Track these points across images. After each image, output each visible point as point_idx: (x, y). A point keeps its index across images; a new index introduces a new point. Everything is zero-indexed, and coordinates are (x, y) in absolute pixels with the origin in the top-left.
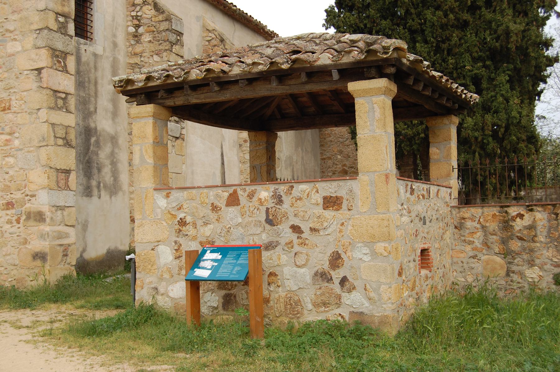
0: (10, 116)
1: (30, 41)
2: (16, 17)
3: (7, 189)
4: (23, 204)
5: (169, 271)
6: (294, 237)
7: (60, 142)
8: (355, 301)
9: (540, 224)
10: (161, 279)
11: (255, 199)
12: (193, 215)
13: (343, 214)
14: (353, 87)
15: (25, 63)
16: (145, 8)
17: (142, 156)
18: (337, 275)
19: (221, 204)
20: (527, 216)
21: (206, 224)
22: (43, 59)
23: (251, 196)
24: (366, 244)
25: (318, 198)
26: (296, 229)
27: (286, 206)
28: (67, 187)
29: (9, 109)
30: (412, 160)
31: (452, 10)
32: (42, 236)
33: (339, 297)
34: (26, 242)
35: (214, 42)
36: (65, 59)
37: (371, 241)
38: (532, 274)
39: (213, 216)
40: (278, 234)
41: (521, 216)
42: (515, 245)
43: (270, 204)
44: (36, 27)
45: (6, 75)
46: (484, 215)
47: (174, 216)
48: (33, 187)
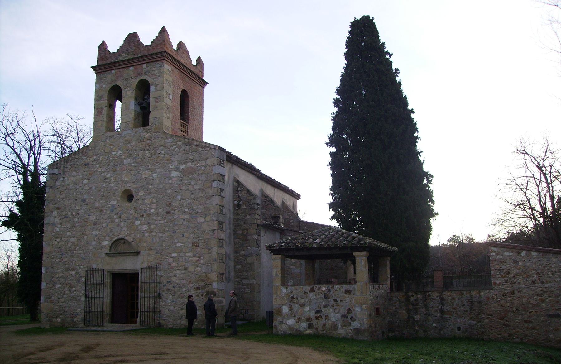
0: (199, 249)
5: (287, 315)
6: (334, 303)
7: (221, 261)
8: (355, 324)
16: (243, 193)
17: (276, 274)
19: (308, 291)
20: (415, 296)
21: (302, 298)
22: (215, 226)
23: (319, 289)
25: (343, 290)
26: (335, 301)
27: (331, 293)
28: (222, 281)
29: (198, 246)
30: (374, 278)
33: (350, 323)
35: (268, 202)
36: (222, 224)
37: (361, 304)
39: (305, 295)
41: (413, 296)
42: (411, 307)
43: (326, 292)
46: (399, 296)
47: (290, 296)
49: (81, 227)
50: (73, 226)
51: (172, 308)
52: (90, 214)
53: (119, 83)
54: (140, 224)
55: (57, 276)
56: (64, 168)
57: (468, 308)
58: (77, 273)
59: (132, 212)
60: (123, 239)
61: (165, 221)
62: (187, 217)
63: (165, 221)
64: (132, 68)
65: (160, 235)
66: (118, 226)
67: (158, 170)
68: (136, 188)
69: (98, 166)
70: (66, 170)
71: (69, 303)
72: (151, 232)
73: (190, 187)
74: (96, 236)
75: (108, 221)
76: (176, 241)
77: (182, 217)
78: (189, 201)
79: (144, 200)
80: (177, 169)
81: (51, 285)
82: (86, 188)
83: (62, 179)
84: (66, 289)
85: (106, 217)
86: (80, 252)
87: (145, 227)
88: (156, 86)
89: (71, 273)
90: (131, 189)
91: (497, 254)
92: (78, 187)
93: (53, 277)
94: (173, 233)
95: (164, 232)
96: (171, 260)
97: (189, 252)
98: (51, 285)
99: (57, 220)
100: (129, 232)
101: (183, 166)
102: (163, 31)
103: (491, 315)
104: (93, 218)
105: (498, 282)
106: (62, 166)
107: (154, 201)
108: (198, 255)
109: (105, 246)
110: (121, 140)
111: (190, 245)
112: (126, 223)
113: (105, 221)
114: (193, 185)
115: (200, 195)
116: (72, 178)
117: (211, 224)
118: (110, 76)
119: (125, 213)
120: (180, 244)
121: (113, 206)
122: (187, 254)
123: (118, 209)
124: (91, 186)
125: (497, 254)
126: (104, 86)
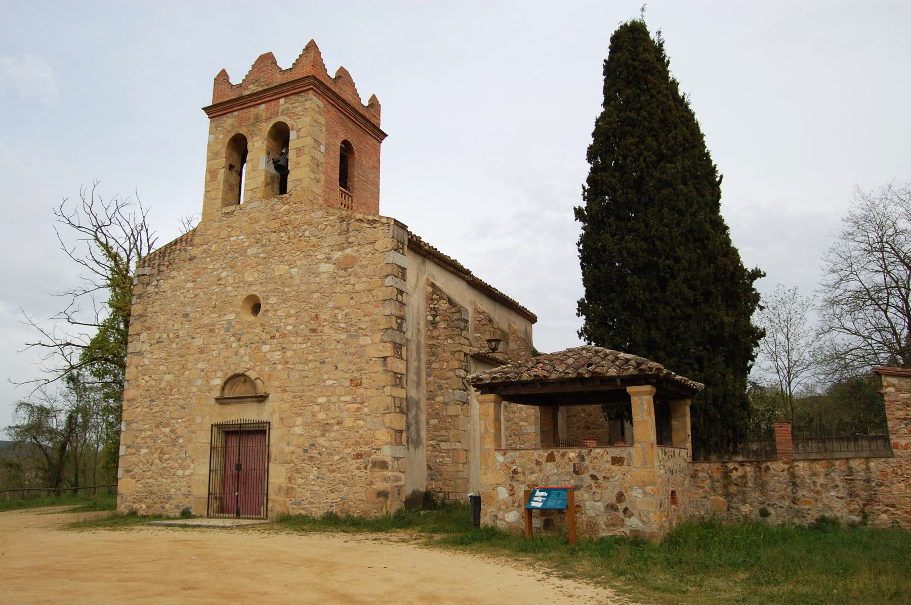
0: (361, 390)
1: (378, 337)
2: (367, 319)
3: (357, 443)
4: (370, 455)
5: (506, 504)
6: (592, 482)
7: (398, 410)
8: (633, 522)
9: (749, 475)
10: (499, 509)
11: (566, 458)
12: (522, 467)
13: (625, 468)
14: (629, 389)
15: (374, 352)
16: (441, 302)
18: (621, 507)
19: (543, 460)
20: (740, 469)
21: (532, 473)
22: (388, 350)
23: (563, 455)
24: (640, 487)
26: (594, 477)
27: (587, 462)
28: (401, 444)
31: (679, 306)
32: (385, 479)
33: (623, 520)
34: (372, 483)
35: (485, 322)
36: (401, 349)
37: (642, 486)
38: (745, 509)
39: (537, 468)
40: (582, 480)
41: (736, 469)
42: (733, 489)
44: (382, 327)
45: (358, 360)
46: (710, 469)
47: (509, 468)
48: (378, 443)
49: (182, 357)
50: (170, 355)
51: (318, 488)
52: (195, 335)
53: (243, 131)
54: (269, 351)
55: (143, 435)
56: (159, 265)
57: (843, 493)
58: (172, 431)
59: (257, 331)
60: (243, 375)
61: (309, 344)
62: (343, 336)
63: (309, 344)
64: (263, 106)
65: (300, 367)
66: (236, 354)
67: (298, 263)
68: (265, 292)
69: (208, 259)
70: (163, 268)
71: (160, 479)
72: (286, 363)
73: (348, 287)
74: (202, 370)
75: (222, 346)
76: (325, 377)
77: (337, 337)
78: (347, 311)
79: (276, 311)
80: (328, 259)
81: (133, 450)
82: (190, 295)
83: (155, 283)
84: (156, 456)
85: (219, 339)
86: (177, 396)
87: (277, 355)
88: (298, 131)
89: (163, 430)
90: (257, 294)
91: (899, 390)
92: (178, 293)
93: (136, 437)
94: (321, 363)
95: (307, 361)
96: (317, 408)
97: (346, 395)
98: (133, 450)
99: (146, 347)
100: (252, 364)
101: (337, 255)
102: (312, 47)
103: (893, 506)
104: (199, 342)
105: (903, 442)
106: (157, 262)
107: (293, 312)
108: (359, 400)
109: (215, 386)
110: (245, 219)
111: (348, 383)
112: (248, 350)
113: (216, 347)
114: (354, 285)
115: (365, 300)
116: (170, 281)
117: (380, 348)
118: (230, 122)
119: (248, 333)
120: (332, 382)
121: (229, 322)
122: (342, 399)
123: (238, 327)
124: (197, 291)
125: (899, 390)
126: (221, 136)
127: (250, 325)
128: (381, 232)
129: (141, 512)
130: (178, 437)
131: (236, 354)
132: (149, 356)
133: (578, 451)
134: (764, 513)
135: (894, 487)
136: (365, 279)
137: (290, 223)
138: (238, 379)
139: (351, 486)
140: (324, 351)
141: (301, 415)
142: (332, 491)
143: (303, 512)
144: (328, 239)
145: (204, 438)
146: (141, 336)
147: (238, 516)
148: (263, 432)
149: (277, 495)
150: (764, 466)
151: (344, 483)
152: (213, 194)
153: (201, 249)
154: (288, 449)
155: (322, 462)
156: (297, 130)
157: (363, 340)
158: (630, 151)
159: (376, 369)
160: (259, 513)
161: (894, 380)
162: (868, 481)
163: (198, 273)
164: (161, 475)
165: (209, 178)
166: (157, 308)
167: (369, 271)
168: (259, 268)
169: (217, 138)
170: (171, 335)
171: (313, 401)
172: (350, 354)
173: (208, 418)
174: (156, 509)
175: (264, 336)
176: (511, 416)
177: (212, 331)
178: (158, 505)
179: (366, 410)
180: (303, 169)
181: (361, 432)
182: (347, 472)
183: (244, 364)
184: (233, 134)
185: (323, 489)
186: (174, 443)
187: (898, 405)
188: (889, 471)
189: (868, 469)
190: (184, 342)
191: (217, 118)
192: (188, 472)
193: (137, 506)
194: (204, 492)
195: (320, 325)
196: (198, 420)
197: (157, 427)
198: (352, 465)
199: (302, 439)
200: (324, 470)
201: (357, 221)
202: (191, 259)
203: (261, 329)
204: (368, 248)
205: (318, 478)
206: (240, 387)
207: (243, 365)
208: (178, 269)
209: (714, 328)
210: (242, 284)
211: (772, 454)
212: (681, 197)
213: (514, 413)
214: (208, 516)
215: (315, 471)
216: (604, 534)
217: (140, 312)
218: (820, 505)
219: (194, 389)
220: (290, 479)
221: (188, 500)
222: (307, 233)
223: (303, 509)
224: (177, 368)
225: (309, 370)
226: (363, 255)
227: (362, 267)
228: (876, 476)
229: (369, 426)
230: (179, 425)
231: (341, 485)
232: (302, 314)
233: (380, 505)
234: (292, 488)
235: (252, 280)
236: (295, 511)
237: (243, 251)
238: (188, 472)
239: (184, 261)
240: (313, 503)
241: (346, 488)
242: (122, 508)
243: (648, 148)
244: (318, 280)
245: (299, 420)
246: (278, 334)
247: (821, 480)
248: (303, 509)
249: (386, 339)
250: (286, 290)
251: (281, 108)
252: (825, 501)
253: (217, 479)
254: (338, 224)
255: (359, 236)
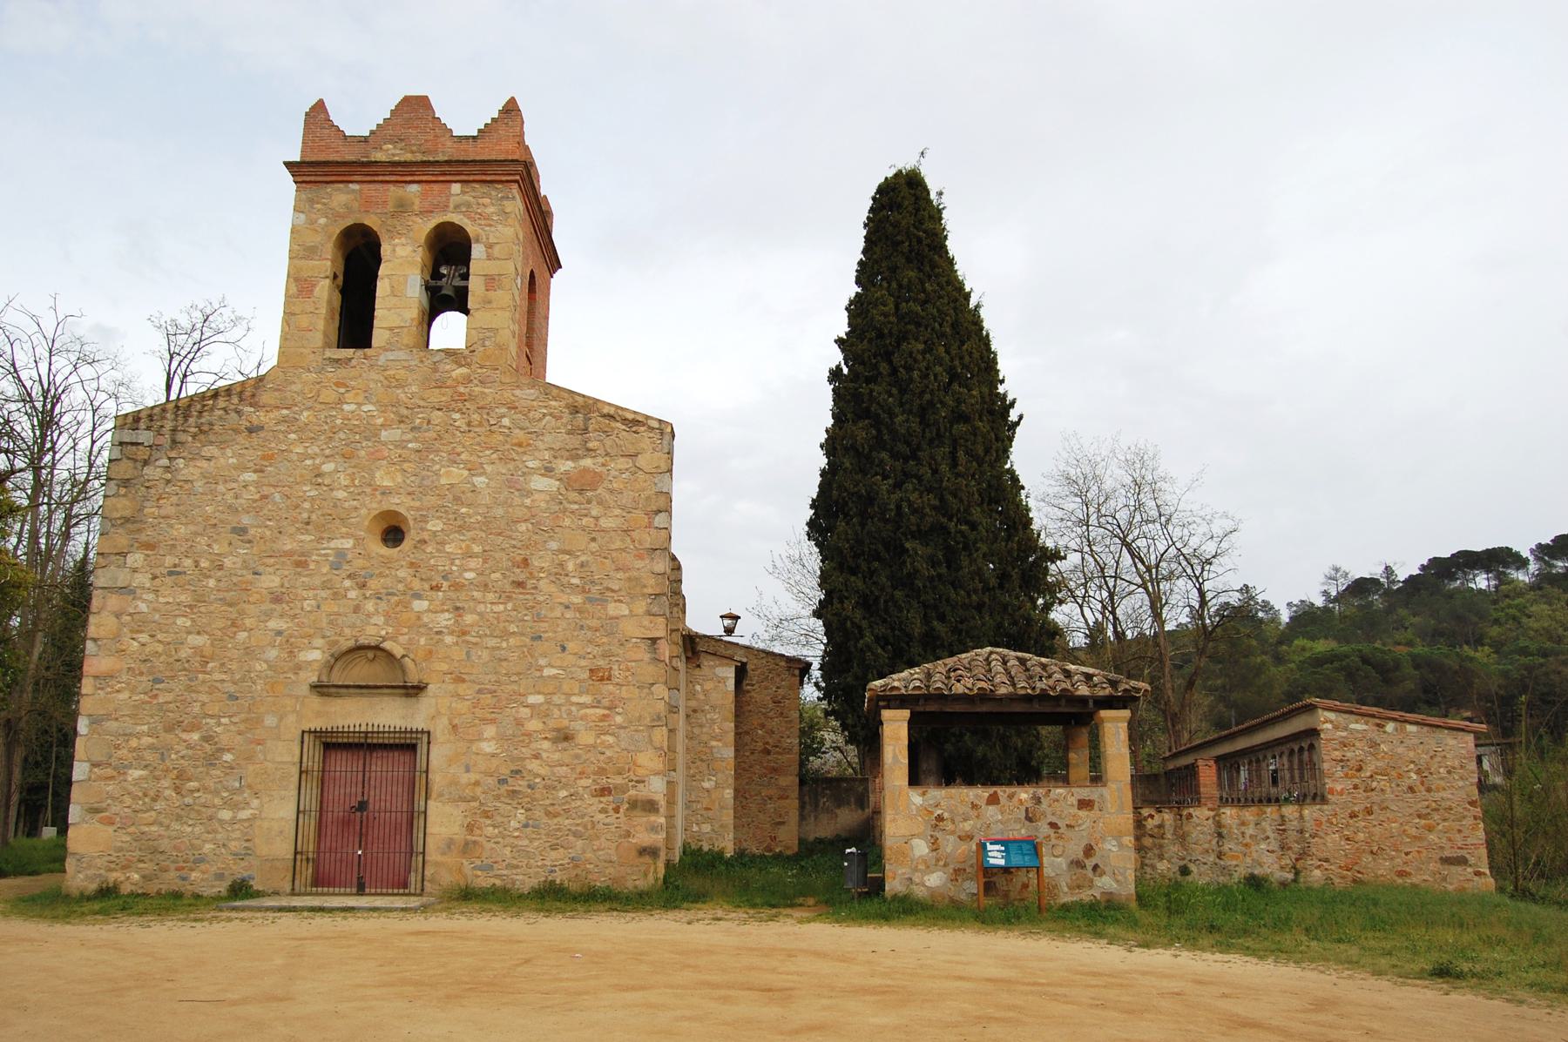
1: (641, 606)
2: (620, 575)
3: (601, 771)
4: (624, 790)
5: (925, 862)
6: (1051, 832)
8: (1105, 883)
9: (1167, 823)
10: (916, 870)
11: (1015, 800)
12: (951, 812)
13: (1094, 814)
14: (1104, 713)
15: (632, 629)
17: (895, 757)
18: (1090, 863)
19: (982, 803)
23: (1011, 797)
24: (1114, 838)
25: (1073, 800)
26: (1053, 825)
27: (1044, 805)
29: (609, 679)
31: (975, 591)
32: (654, 829)
34: (628, 834)
38: (1162, 866)
39: (973, 813)
40: (1037, 829)
41: (1152, 816)
42: (1147, 841)
43: (1029, 805)
44: (650, 591)
45: (605, 640)
48: (640, 772)
49: (230, 605)
50: (200, 599)
51: (526, 842)
52: (261, 569)
53: (371, 221)
54: (429, 611)
55: (134, 743)
56: (174, 430)
57: (1274, 845)
58: (207, 739)
59: (401, 574)
60: (377, 648)
61: (510, 606)
62: (577, 599)
63: (510, 606)
64: (414, 188)
65: (492, 642)
66: (357, 609)
67: (489, 468)
68: (418, 509)
69: (293, 436)
70: (181, 437)
71: (176, 826)
72: (464, 633)
73: (585, 521)
74: (279, 633)
75: (324, 594)
76: (542, 662)
77: (564, 599)
78: (583, 558)
79: (443, 543)
80: (548, 471)
81: (109, 772)
82: (252, 494)
83: (165, 462)
84: (165, 783)
85: (317, 581)
86: (217, 676)
87: (445, 619)
88: (490, 246)
89: (184, 736)
90: (402, 510)
91: (1336, 728)
92: (221, 488)
93: (117, 747)
94: (533, 639)
95: (506, 635)
96: (525, 712)
97: (580, 694)
98: (109, 772)
99: (143, 579)
100: (390, 630)
101: (568, 465)
102: (511, 110)
103: (1327, 860)
104: (270, 581)
105: (1339, 788)
106: (169, 425)
107: (477, 549)
108: (605, 702)
109: (310, 663)
110: (373, 375)
111: (586, 675)
112: (383, 606)
113: (311, 593)
114: (597, 519)
115: (618, 544)
116: (204, 464)
117: (646, 623)
119: (381, 575)
120: (554, 671)
121: (341, 553)
122: (574, 699)
123: (360, 562)
124: (266, 490)
125: (1336, 728)
126: (323, 221)
127: (387, 562)
128: (648, 441)
129: (126, 889)
130: (221, 750)
131: (357, 609)
132: (151, 597)
133: (1032, 791)
134: (1185, 871)
135: (1328, 839)
136: (617, 512)
137: (471, 398)
138: (362, 653)
139: (590, 839)
140: (539, 618)
141: (493, 721)
142: (554, 847)
143: (498, 882)
144: (548, 438)
145: (285, 754)
146: (130, 559)
147: (361, 890)
148: (411, 748)
149: (443, 854)
150: (1185, 813)
151: (576, 835)
152: (304, 321)
153: (275, 414)
154: (465, 778)
155: (534, 800)
156: (416, 226)
157: (613, 609)
158: (916, 361)
159: (639, 656)
160: (405, 886)
161: (1331, 715)
162: (1301, 832)
163: (268, 457)
164: (179, 818)
165: (294, 290)
166: (171, 510)
167: (626, 499)
168: (405, 466)
169: (313, 222)
170: (204, 564)
171: (518, 698)
172: (590, 628)
173: (292, 718)
174: (170, 881)
175: (416, 585)
176: (696, 731)
177: (301, 564)
178: (173, 874)
179: (619, 719)
180: (499, 313)
181: (609, 753)
182: (582, 817)
183: (374, 629)
184: (349, 222)
185: (536, 844)
186: (211, 761)
187: (1335, 744)
188: (1324, 820)
189: (1301, 817)
190: (235, 579)
191: (314, 187)
192: (245, 814)
193: (114, 876)
194: (284, 849)
195: (531, 576)
196: (270, 721)
197: (169, 729)
198: (592, 805)
199: (495, 762)
200: (538, 813)
201: (604, 416)
202: (251, 430)
203: (411, 571)
204: (623, 463)
205: (526, 826)
206: (371, 666)
207: (371, 630)
208: (223, 445)
209: (1015, 623)
210: (368, 490)
211: (1198, 801)
212: (980, 439)
213: (701, 726)
214: (293, 893)
215: (521, 814)
216: (1066, 899)
217: (127, 513)
218: (1248, 860)
219: (260, 666)
220: (470, 828)
221: (243, 864)
222: (506, 421)
223: (496, 876)
224: (220, 624)
225: (509, 648)
226: (613, 473)
227: (611, 491)
228: (1309, 826)
229: (623, 745)
230: (224, 731)
231: (571, 838)
232: (498, 555)
233: (643, 868)
234: (475, 842)
235: (392, 486)
236: (483, 881)
237: (372, 433)
238: (245, 814)
239: (237, 431)
240: (517, 867)
241: (580, 843)
242: (78, 878)
243: (939, 361)
244: (528, 502)
245: (490, 731)
246: (445, 584)
247: (1250, 831)
248: (496, 876)
249: (655, 609)
250: (464, 510)
251: (453, 201)
252: (1255, 855)
253: (310, 824)
254: (566, 417)
255: (608, 442)
